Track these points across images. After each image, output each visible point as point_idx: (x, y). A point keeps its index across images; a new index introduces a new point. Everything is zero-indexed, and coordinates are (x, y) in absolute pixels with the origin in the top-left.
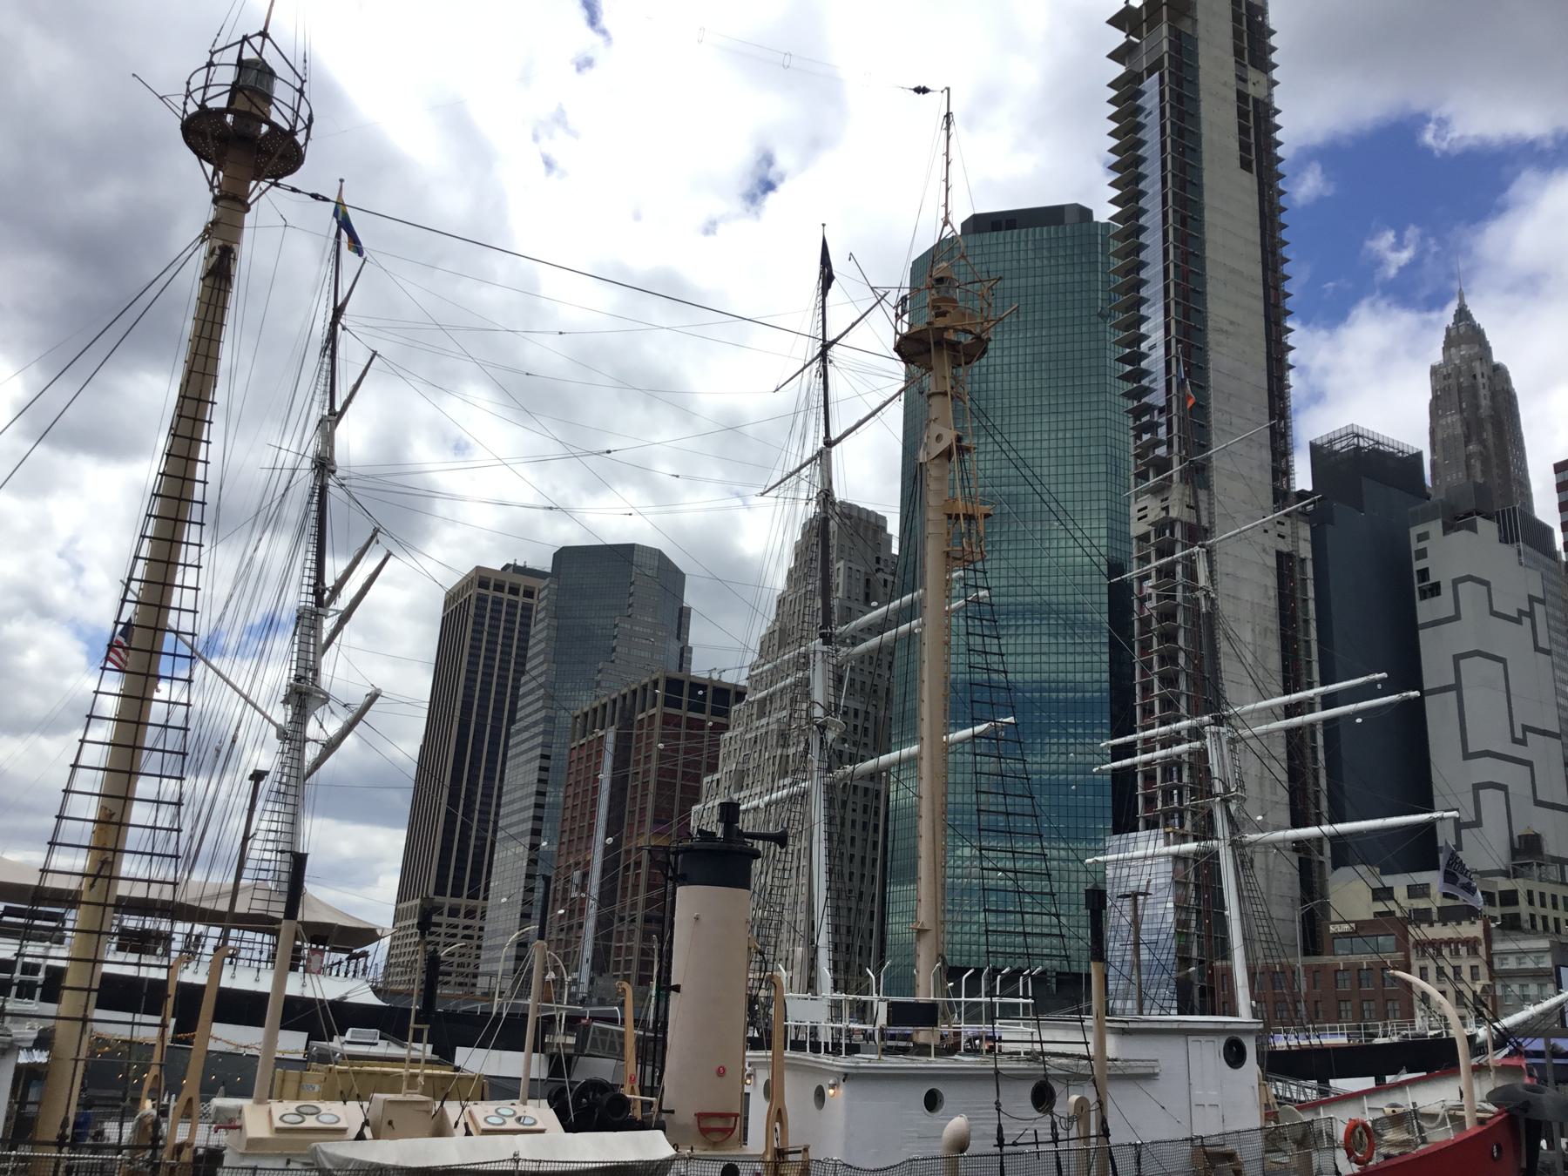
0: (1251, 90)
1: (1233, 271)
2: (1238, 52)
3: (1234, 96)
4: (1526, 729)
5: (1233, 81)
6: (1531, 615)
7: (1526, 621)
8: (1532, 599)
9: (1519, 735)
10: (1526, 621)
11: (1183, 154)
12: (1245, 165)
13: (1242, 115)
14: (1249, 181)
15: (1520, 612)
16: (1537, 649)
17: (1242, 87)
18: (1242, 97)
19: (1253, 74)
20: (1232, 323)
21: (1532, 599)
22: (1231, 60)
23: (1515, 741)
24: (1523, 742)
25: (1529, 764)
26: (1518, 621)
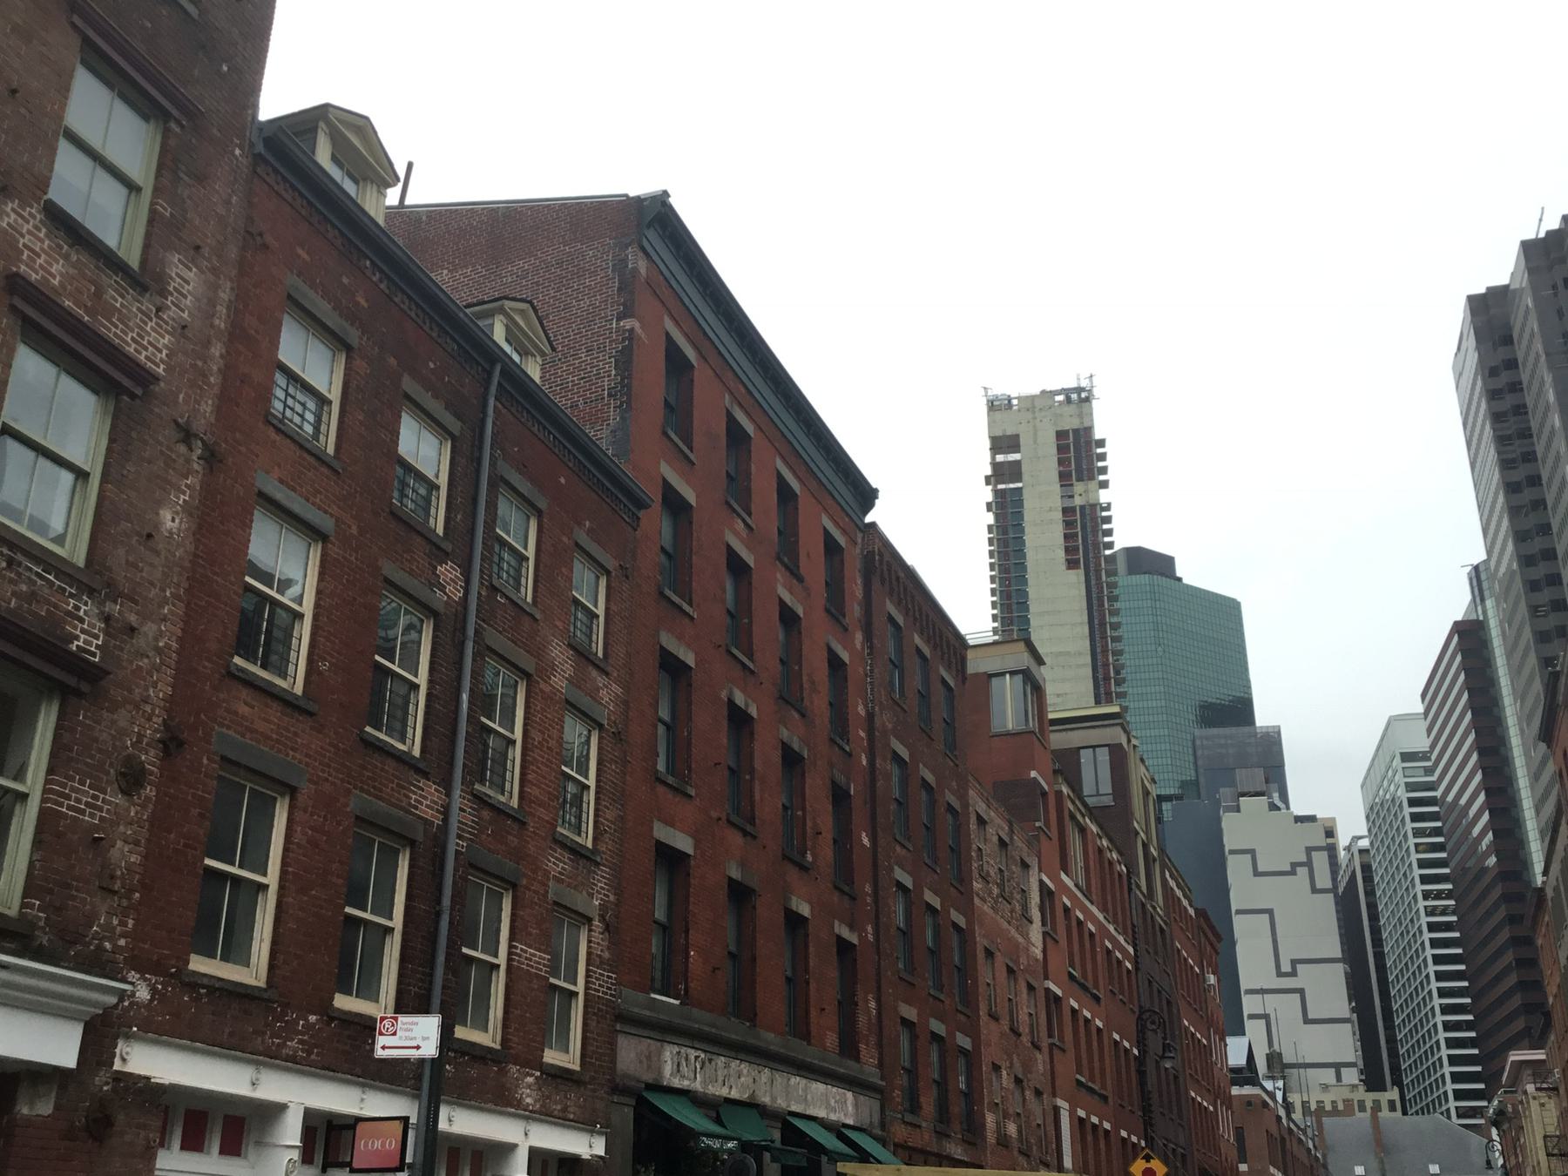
0: (1078, 501)
1: (1060, 654)
2: (1064, 478)
3: (1059, 515)
4: (1294, 962)
5: (1058, 503)
6: (1309, 864)
7: (1302, 872)
8: (1309, 850)
9: (1286, 968)
10: (1302, 872)
11: (1009, 585)
12: (1072, 564)
13: (1068, 524)
14: (1077, 577)
15: (1294, 865)
16: (1314, 890)
17: (1068, 503)
18: (1065, 511)
19: (1079, 487)
20: (1058, 695)
21: (1309, 850)
22: (1056, 487)
23: (1280, 974)
24: (1294, 973)
25: (1301, 992)
26: (1293, 872)
